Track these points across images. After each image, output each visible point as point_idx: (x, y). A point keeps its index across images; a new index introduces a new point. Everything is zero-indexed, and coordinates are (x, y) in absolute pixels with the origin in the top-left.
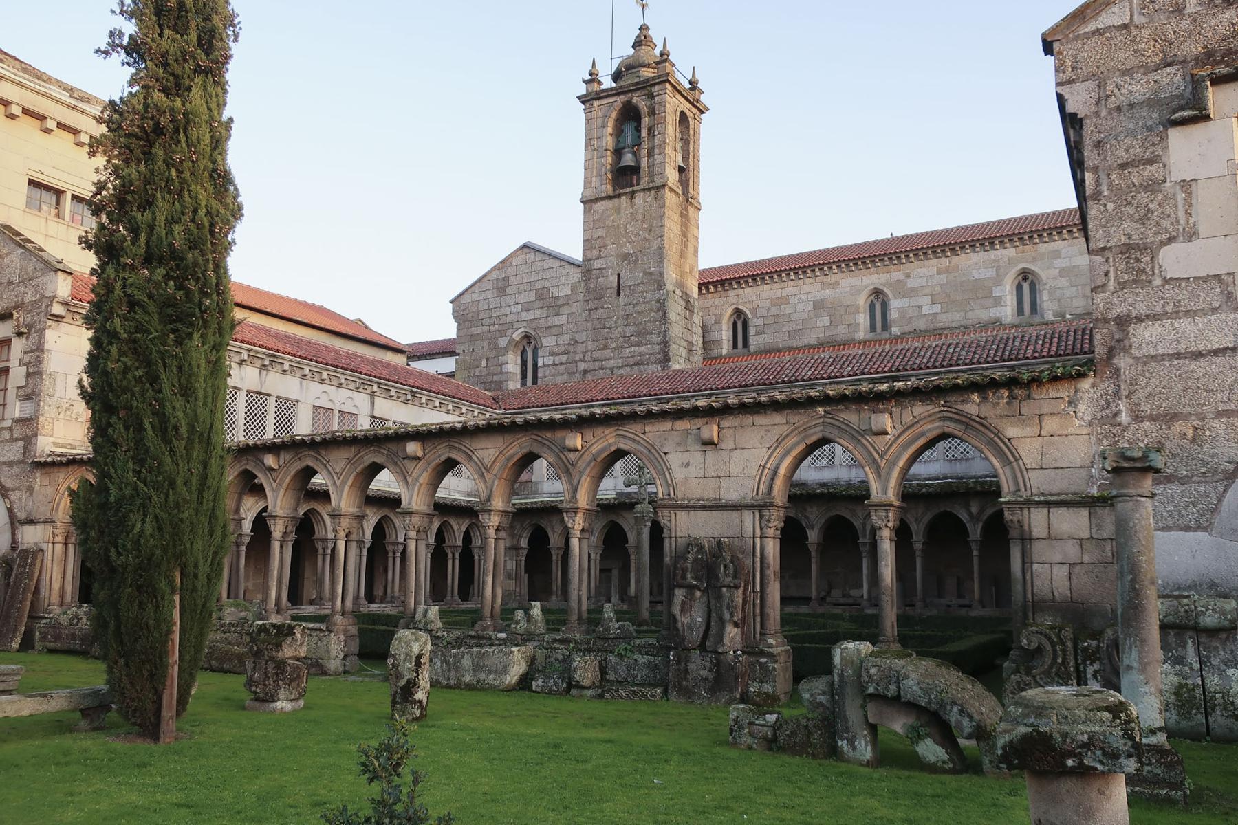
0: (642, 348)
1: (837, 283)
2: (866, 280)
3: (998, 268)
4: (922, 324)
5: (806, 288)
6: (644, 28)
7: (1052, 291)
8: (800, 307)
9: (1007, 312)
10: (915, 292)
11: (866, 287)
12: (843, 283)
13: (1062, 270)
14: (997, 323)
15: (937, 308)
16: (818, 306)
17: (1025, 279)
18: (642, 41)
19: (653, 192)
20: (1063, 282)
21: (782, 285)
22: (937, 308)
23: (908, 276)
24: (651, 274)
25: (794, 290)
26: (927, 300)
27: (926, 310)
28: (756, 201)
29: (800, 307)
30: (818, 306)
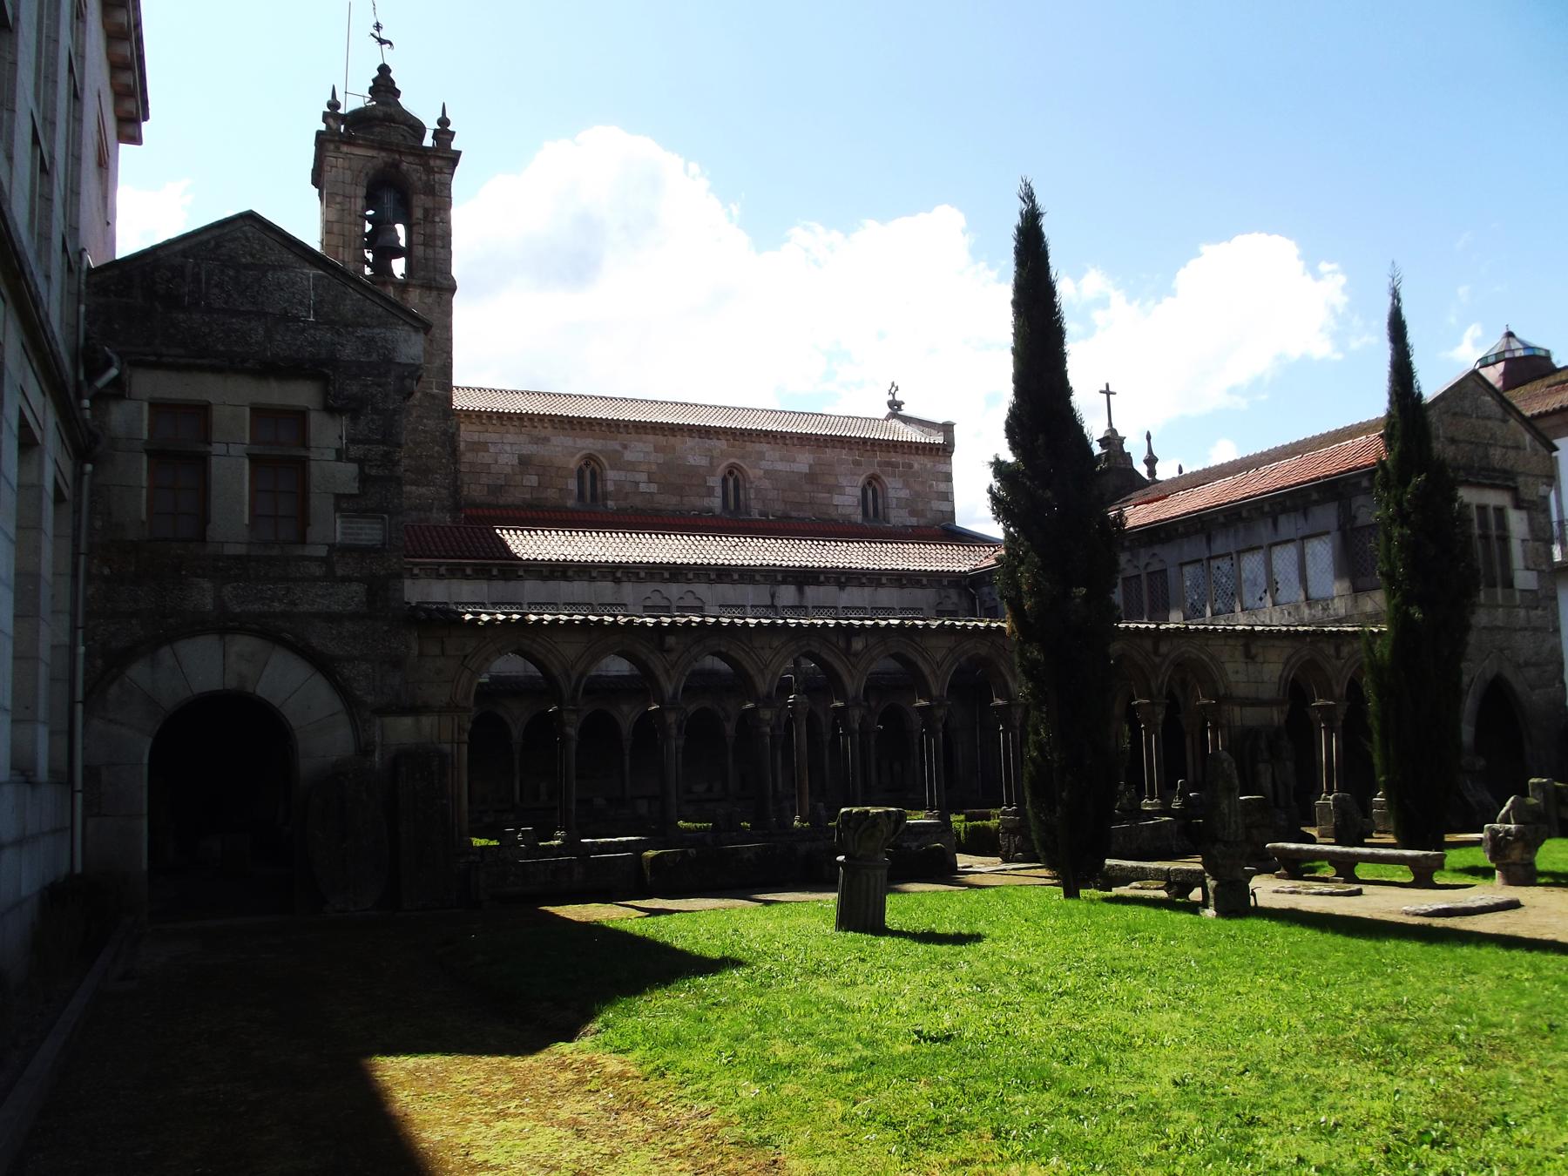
0: (423, 490)
1: (546, 440)
2: (580, 443)
3: (712, 458)
4: (638, 502)
5: (510, 438)
6: (384, 70)
7: (758, 490)
8: (503, 459)
9: (716, 503)
10: (632, 467)
11: (580, 450)
12: (555, 441)
13: (766, 472)
14: (710, 510)
15: (653, 488)
16: (525, 462)
17: (731, 473)
18: (384, 85)
19: (434, 293)
20: (767, 484)
21: (480, 428)
22: (653, 488)
23: (625, 447)
24: (433, 396)
25: (493, 437)
26: (644, 477)
27: (643, 487)
28: (1186, 471)
29: (503, 459)
30: (525, 462)
